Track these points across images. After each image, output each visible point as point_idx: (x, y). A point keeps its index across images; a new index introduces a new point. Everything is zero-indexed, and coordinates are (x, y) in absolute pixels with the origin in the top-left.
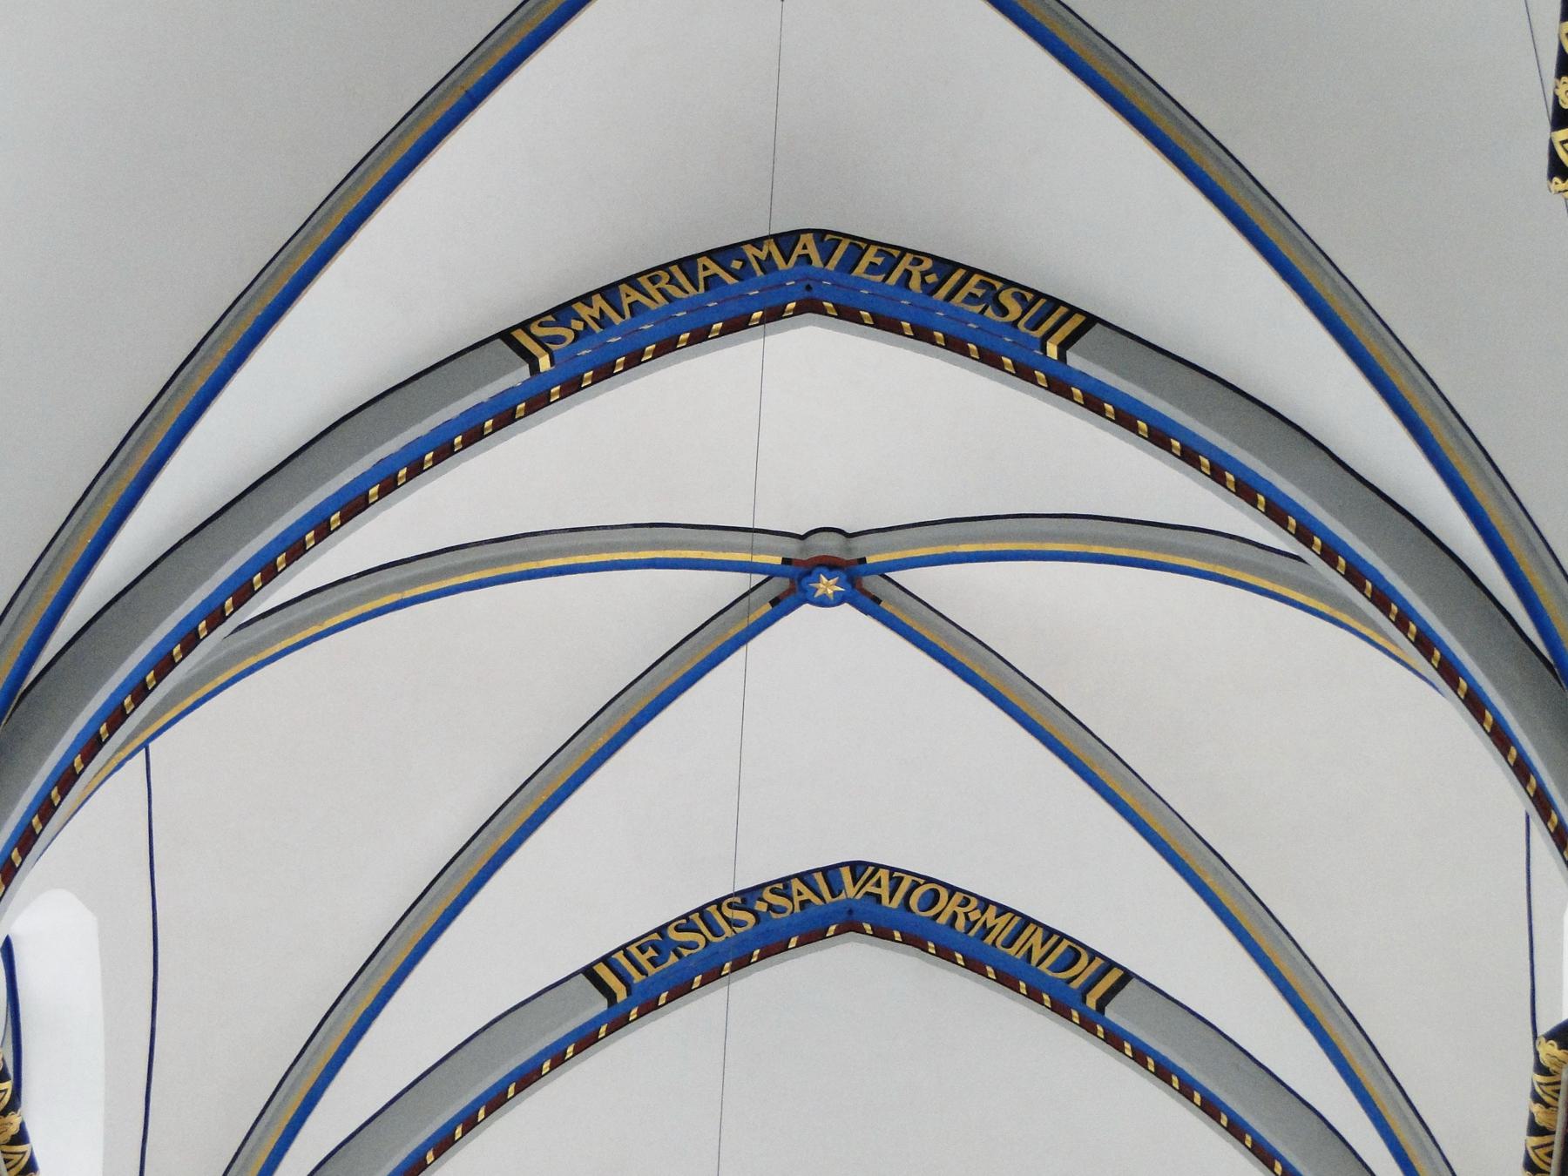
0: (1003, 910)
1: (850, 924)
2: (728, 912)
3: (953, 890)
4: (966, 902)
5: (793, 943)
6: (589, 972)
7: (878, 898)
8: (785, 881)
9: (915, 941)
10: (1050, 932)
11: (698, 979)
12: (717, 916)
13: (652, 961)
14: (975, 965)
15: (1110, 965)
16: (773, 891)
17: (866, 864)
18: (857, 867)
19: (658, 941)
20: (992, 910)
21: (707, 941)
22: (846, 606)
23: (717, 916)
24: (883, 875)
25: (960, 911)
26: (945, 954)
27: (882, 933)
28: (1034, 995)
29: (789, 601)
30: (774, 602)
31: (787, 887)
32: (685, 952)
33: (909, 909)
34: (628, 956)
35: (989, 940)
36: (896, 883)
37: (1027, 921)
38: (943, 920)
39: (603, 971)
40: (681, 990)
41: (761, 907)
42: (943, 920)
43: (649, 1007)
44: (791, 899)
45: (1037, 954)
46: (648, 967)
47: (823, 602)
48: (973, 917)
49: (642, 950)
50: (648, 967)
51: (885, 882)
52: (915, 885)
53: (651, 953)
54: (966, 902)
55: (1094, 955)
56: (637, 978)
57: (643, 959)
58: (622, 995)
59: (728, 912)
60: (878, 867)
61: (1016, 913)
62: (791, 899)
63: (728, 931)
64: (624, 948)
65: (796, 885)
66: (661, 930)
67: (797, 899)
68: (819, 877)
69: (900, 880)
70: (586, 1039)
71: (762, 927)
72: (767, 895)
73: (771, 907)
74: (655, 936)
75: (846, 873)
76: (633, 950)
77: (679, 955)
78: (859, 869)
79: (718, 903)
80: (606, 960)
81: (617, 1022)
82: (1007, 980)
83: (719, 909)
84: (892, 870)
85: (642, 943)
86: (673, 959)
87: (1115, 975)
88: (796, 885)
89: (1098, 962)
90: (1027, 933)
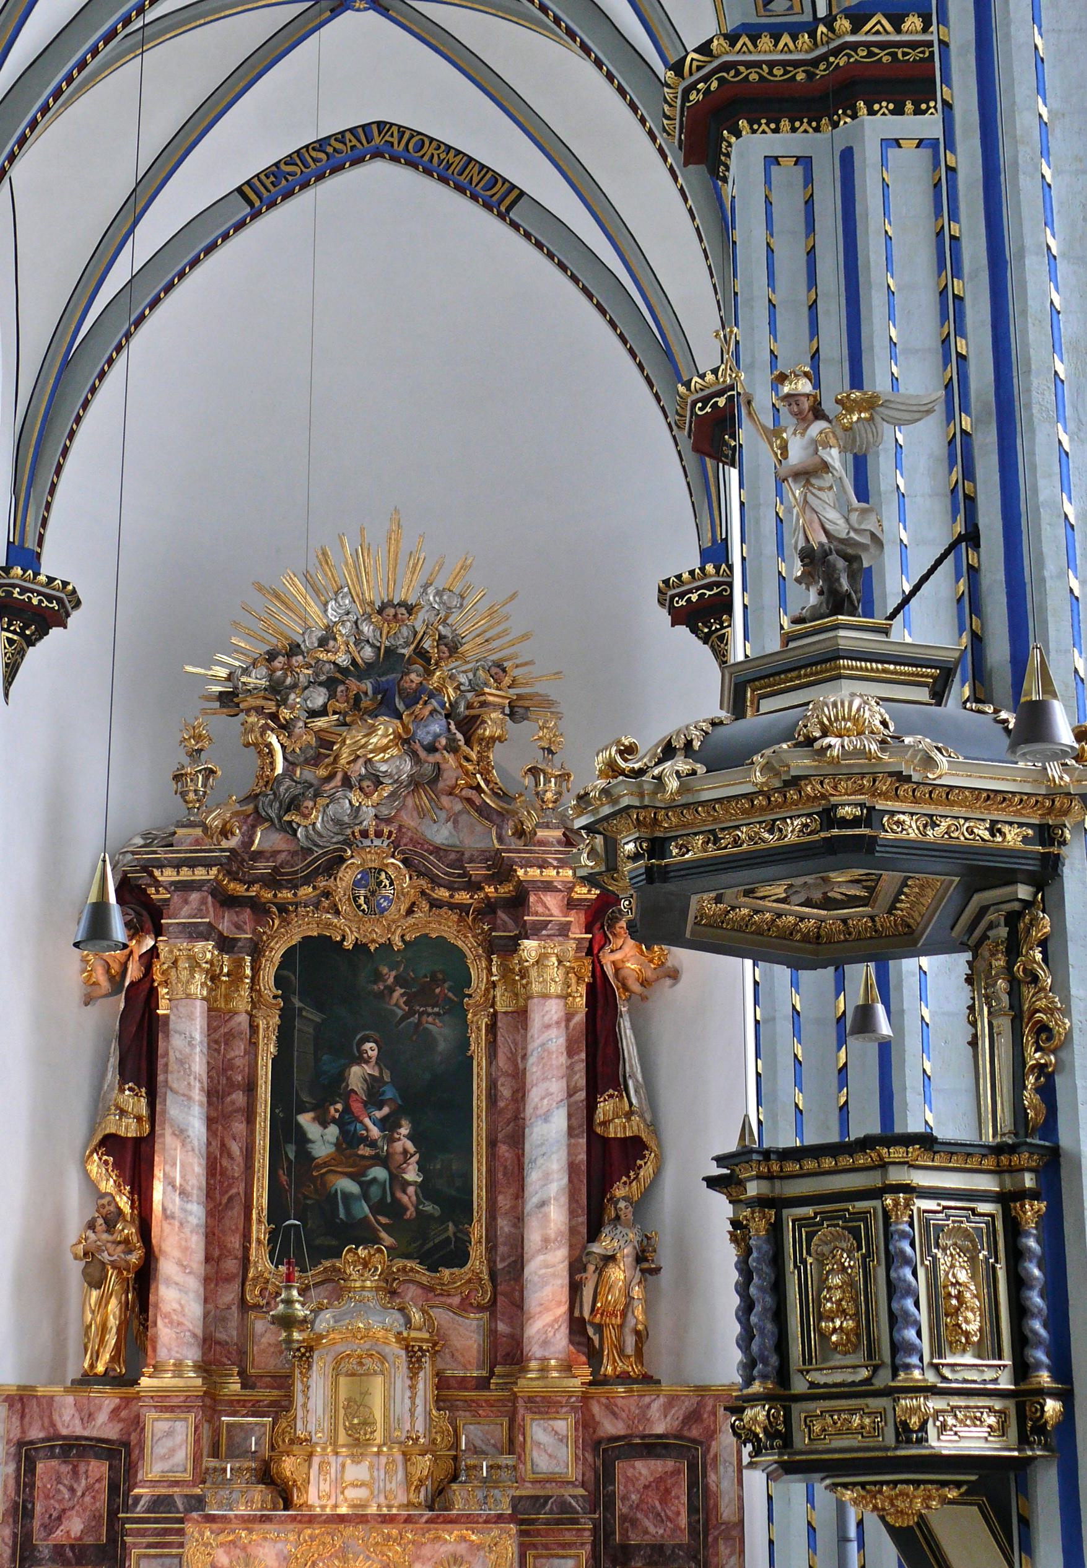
0: (458, 152)
1: (377, 154)
2: (314, 154)
3: (432, 140)
4: (439, 148)
5: (347, 165)
6: (239, 190)
7: (392, 144)
8: (343, 133)
9: (412, 164)
10: (483, 166)
11: (297, 188)
12: (307, 155)
13: (272, 183)
14: (443, 180)
15: (513, 187)
16: (336, 140)
17: (386, 123)
18: (380, 124)
19: (275, 172)
20: (452, 152)
21: (302, 172)
22: (371, 11)
23: (307, 155)
24: (395, 129)
25: (436, 153)
26: (428, 172)
27: (395, 159)
28: (474, 197)
29: (339, 10)
30: (332, 11)
31: (343, 137)
32: (290, 178)
33: (408, 151)
34: (259, 180)
35: (450, 171)
36: (402, 135)
37: (471, 159)
38: (426, 158)
39: (247, 190)
40: (288, 195)
41: (330, 150)
42: (426, 158)
43: (272, 205)
44: (345, 144)
45: (475, 180)
46: (270, 187)
47: (358, 10)
48: (442, 156)
49: (267, 177)
50: (270, 187)
51: (396, 134)
52: (412, 137)
53: (272, 178)
54: (439, 148)
55: (505, 180)
56: (265, 194)
57: (267, 182)
58: (257, 204)
59: (314, 154)
60: (392, 125)
61: (465, 155)
62: (345, 144)
63: (313, 166)
64: (257, 175)
65: (348, 135)
66: (277, 164)
67: (349, 145)
68: (360, 130)
69: (404, 132)
70: (240, 226)
71: (331, 161)
72: (333, 142)
73: (335, 150)
74: (274, 168)
75: (374, 127)
76: (262, 177)
77: (287, 180)
78: (382, 126)
79: (307, 147)
80: (248, 183)
81: (256, 215)
82: (460, 189)
83: (307, 151)
84: (400, 127)
85: (267, 172)
86: (284, 182)
87: (516, 193)
88: (348, 135)
89: (507, 185)
90: (470, 166)
